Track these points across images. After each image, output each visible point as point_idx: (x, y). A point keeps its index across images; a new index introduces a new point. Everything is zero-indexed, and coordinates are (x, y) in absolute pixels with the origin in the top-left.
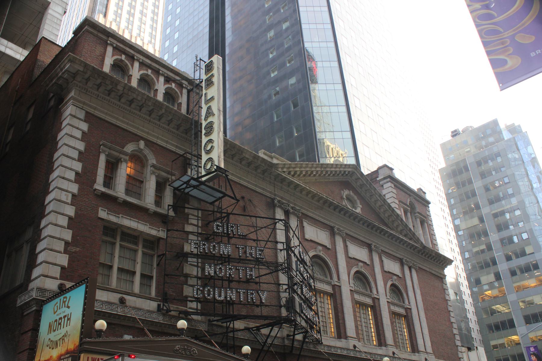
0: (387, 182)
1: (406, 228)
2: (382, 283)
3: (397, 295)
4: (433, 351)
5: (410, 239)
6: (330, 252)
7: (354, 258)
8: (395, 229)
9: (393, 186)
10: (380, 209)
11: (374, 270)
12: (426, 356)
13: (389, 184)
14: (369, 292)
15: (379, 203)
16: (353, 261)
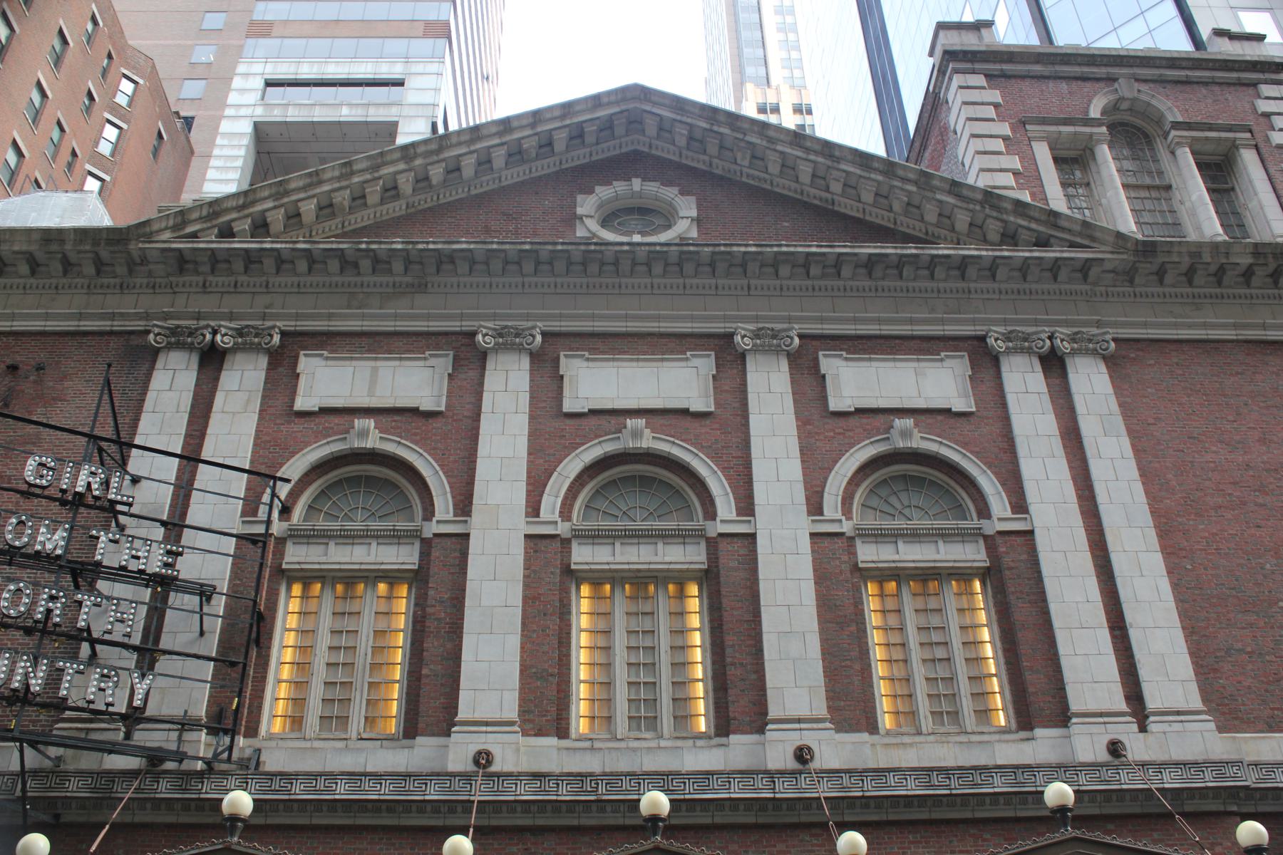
0: (950, 79)
2: (793, 469)
3: (948, 492)
4: (1205, 700)
5: (1042, 242)
6: (436, 424)
7: (593, 412)
8: (943, 232)
9: (980, 80)
10: (827, 190)
11: (746, 425)
12: (1126, 732)
13: (957, 80)
14: (699, 521)
15: (805, 171)
16: (593, 421)
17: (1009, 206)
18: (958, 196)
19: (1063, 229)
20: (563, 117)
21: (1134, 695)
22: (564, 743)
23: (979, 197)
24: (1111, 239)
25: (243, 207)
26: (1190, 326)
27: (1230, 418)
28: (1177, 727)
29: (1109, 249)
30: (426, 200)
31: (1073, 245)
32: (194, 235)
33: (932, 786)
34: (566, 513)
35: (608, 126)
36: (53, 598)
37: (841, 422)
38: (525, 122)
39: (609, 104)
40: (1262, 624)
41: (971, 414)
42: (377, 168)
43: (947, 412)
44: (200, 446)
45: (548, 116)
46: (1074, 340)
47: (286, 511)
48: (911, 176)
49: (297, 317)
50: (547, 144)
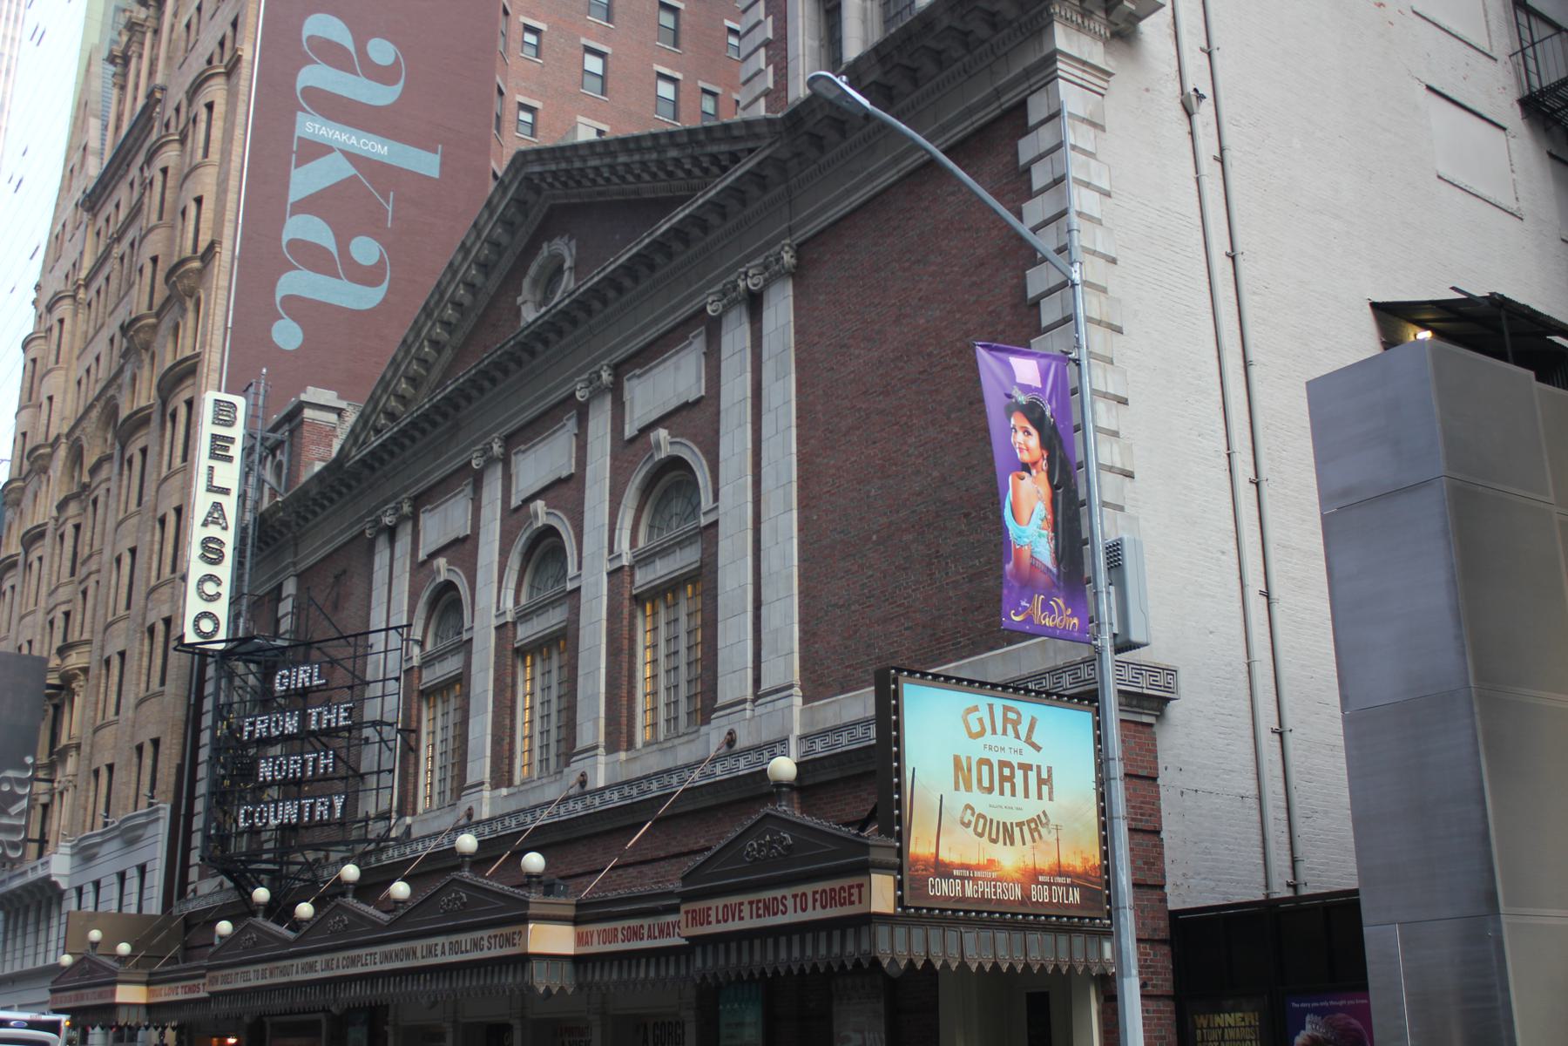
1: (698, 143)
5: (735, 158)
6: (468, 546)
17: (702, 137)
18: (677, 145)
19: (736, 139)
20: (491, 216)
21: (757, 681)
22: (512, 790)
23: (685, 139)
24: (764, 130)
25: (375, 408)
26: (856, 188)
27: (876, 301)
28: (770, 707)
29: (768, 141)
30: (459, 337)
31: (751, 151)
32: (364, 443)
33: (625, 798)
34: (517, 601)
35: (520, 203)
36: (296, 762)
37: (638, 444)
38: (472, 238)
39: (511, 182)
40: (855, 568)
41: (702, 398)
42: (418, 335)
43: (686, 406)
44: (368, 621)
45: (482, 222)
46: (766, 268)
47: (422, 644)
48: (649, 144)
49: (417, 481)
50: (495, 245)
